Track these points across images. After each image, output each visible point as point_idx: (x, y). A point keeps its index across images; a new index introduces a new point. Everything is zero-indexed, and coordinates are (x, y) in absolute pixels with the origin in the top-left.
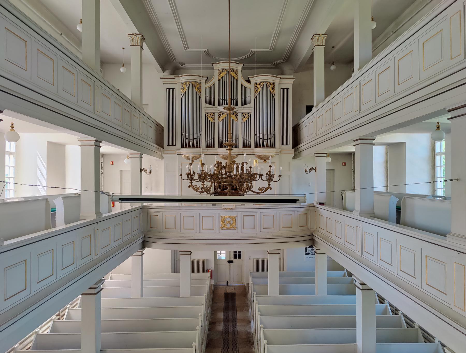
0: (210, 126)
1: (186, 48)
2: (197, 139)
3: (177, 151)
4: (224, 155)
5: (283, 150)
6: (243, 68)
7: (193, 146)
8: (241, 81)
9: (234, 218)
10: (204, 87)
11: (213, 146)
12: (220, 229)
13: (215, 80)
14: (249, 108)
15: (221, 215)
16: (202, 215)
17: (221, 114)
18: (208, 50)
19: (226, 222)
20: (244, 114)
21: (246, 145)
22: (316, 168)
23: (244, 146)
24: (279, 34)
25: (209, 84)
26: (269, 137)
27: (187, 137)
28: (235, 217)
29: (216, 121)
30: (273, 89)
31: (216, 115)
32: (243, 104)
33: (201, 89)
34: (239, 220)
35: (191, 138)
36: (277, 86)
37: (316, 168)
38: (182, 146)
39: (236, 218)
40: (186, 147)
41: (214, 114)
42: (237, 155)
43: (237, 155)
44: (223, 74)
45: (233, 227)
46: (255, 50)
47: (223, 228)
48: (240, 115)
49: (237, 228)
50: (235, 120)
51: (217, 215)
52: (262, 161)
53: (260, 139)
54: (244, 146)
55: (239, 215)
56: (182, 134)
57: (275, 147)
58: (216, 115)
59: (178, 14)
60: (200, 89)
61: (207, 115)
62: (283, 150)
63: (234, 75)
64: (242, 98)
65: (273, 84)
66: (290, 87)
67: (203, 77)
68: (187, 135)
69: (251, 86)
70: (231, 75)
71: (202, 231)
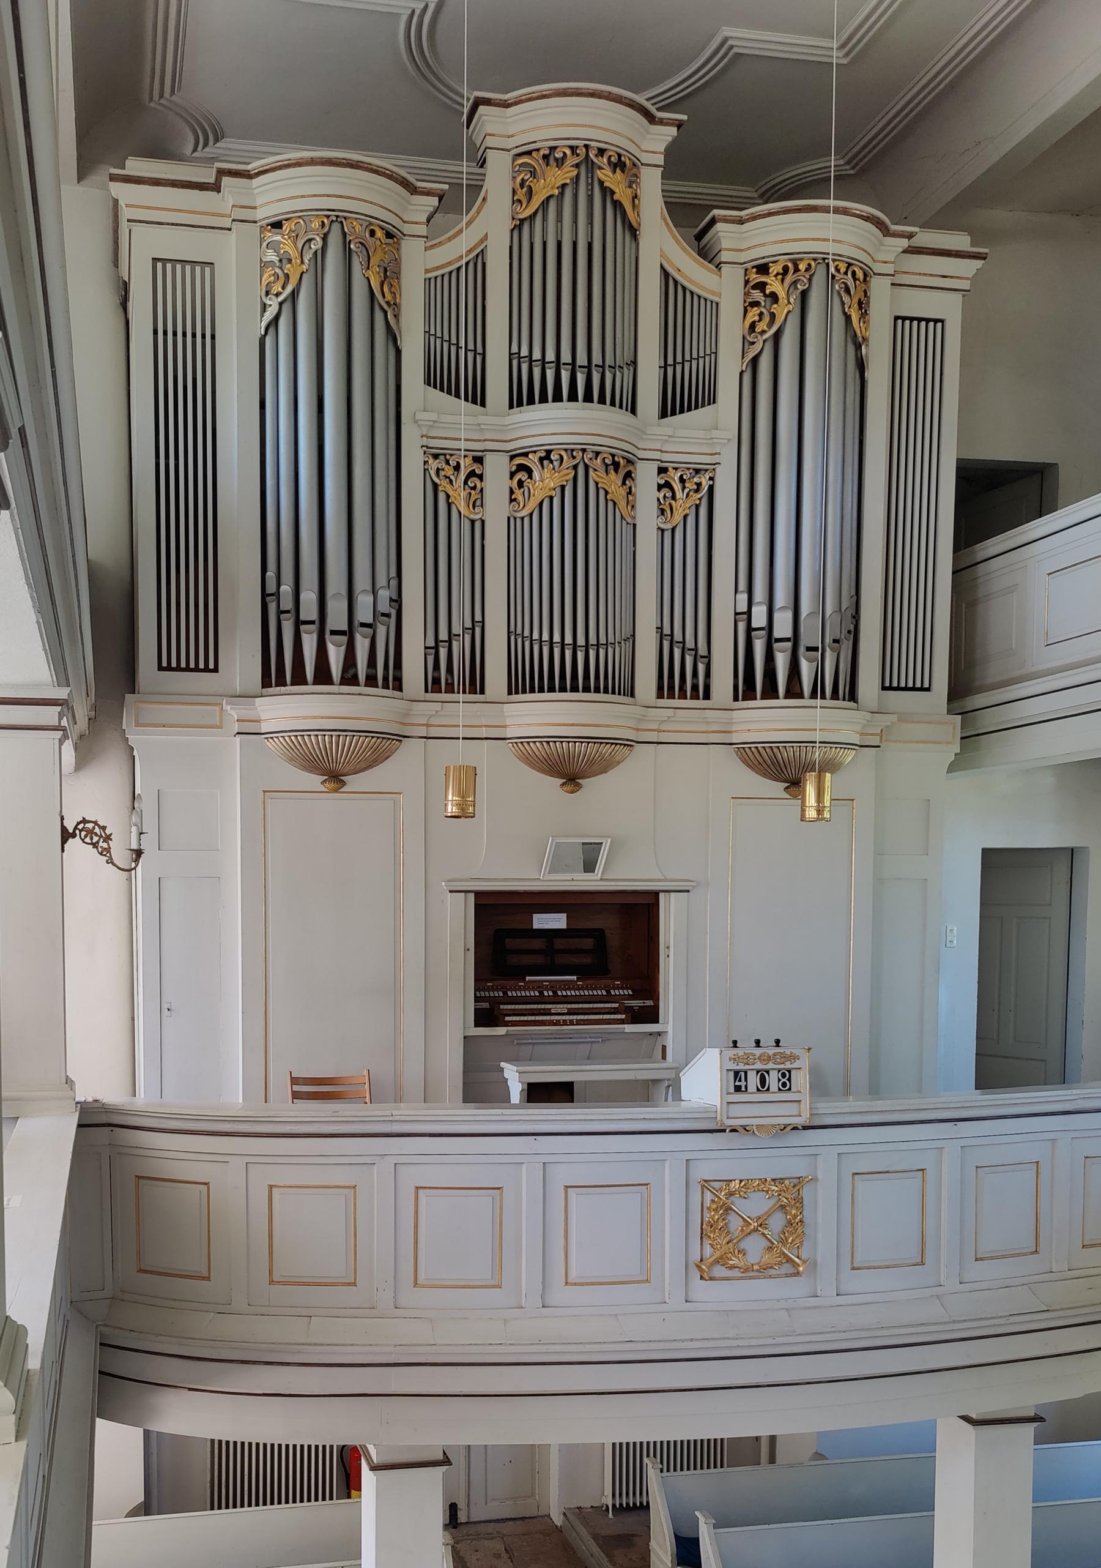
3: (233, 711)
4: (549, 739)
5: (904, 718)
6: (676, 164)
7: (349, 678)
8: (660, 243)
9: (791, 1195)
10: (418, 262)
13: (491, 223)
14: (709, 435)
15: (703, 1171)
17: (532, 461)
19: (735, 1224)
20: (674, 477)
21: (682, 682)
23: (666, 688)
25: (455, 250)
29: (496, 511)
31: (497, 470)
33: (397, 275)
38: (276, 674)
39: (806, 1193)
40: (299, 678)
41: (479, 460)
42: (628, 744)
44: (554, 178)
45: (786, 1257)
46: (745, 37)
50: (622, 504)
54: (666, 688)
58: (497, 470)
60: (391, 274)
61: (434, 464)
62: (904, 718)
63: (622, 194)
66: (948, 308)
67: (413, 190)
70: (607, 192)
71: (560, 1294)
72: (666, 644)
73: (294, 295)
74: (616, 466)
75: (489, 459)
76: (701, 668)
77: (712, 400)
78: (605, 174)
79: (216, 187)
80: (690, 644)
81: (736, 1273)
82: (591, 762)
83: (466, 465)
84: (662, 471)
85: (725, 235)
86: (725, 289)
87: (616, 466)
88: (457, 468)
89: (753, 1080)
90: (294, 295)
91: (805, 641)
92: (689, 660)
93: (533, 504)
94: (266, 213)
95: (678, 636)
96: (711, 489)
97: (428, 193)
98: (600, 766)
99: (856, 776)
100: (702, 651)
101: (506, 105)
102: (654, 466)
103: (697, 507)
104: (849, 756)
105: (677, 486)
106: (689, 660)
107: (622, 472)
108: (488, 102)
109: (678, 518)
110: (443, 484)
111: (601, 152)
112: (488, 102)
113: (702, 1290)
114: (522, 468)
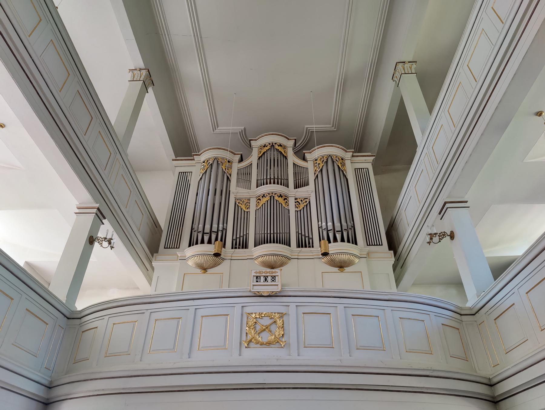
0: (241, 216)
1: (215, 125)
2: (217, 232)
8: (292, 159)
10: (236, 166)
11: (245, 246)
12: (244, 350)
13: (254, 159)
14: (308, 191)
15: (248, 310)
16: (200, 313)
17: (261, 198)
18: (245, 129)
19: (258, 328)
21: (304, 243)
22: (452, 232)
23: (300, 245)
24: (344, 85)
26: (344, 227)
27: (201, 229)
28: (282, 315)
30: (344, 165)
31: (253, 202)
32: (296, 187)
34: (291, 322)
35: (207, 229)
36: (348, 163)
37: (452, 232)
41: (249, 200)
42: (289, 259)
43: (289, 259)
47: (252, 345)
48: (292, 201)
49: (287, 345)
51: (237, 310)
52: (336, 269)
53: (328, 231)
54: (300, 245)
55: (292, 310)
56: (192, 229)
57: (356, 244)
58: (253, 202)
59: (201, 37)
64: (295, 181)
65: (342, 159)
66: (370, 166)
67: (235, 154)
68: (201, 226)
69: (309, 165)
72: (300, 236)
73: (206, 171)
74: (282, 197)
75: (251, 199)
76: (311, 241)
77: (308, 185)
78: (277, 147)
79: (194, 160)
80: (307, 235)
81: (258, 345)
82: (275, 262)
83: (246, 201)
84: (295, 199)
85: (307, 156)
86: (309, 165)
87: (282, 197)
88: (243, 202)
89: (262, 279)
90: (206, 171)
91: (337, 229)
92: (307, 239)
93: (261, 205)
94: (202, 161)
95: (303, 234)
96: (310, 202)
97: (238, 154)
98: (282, 265)
99: (360, 265)
100: (311, 236)
101: (256, 140)
102: (294, 198)
103: (307, 206)
104: (357, 260)
105: (300, 202)
106: (307, 239)
107: (283, 198)
108: (252, 140)
109: (301, 208)
110: (240, 205)
111: (275, 144)
112: (252, 140)
113: (244, 350)
114: (260, 199)
